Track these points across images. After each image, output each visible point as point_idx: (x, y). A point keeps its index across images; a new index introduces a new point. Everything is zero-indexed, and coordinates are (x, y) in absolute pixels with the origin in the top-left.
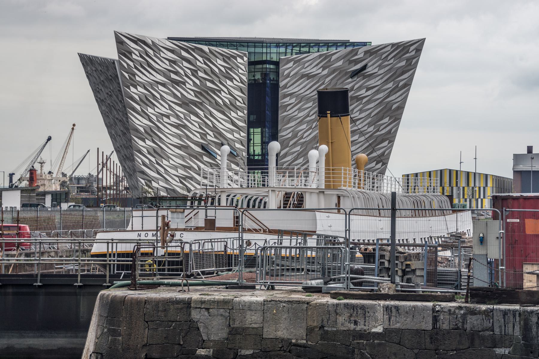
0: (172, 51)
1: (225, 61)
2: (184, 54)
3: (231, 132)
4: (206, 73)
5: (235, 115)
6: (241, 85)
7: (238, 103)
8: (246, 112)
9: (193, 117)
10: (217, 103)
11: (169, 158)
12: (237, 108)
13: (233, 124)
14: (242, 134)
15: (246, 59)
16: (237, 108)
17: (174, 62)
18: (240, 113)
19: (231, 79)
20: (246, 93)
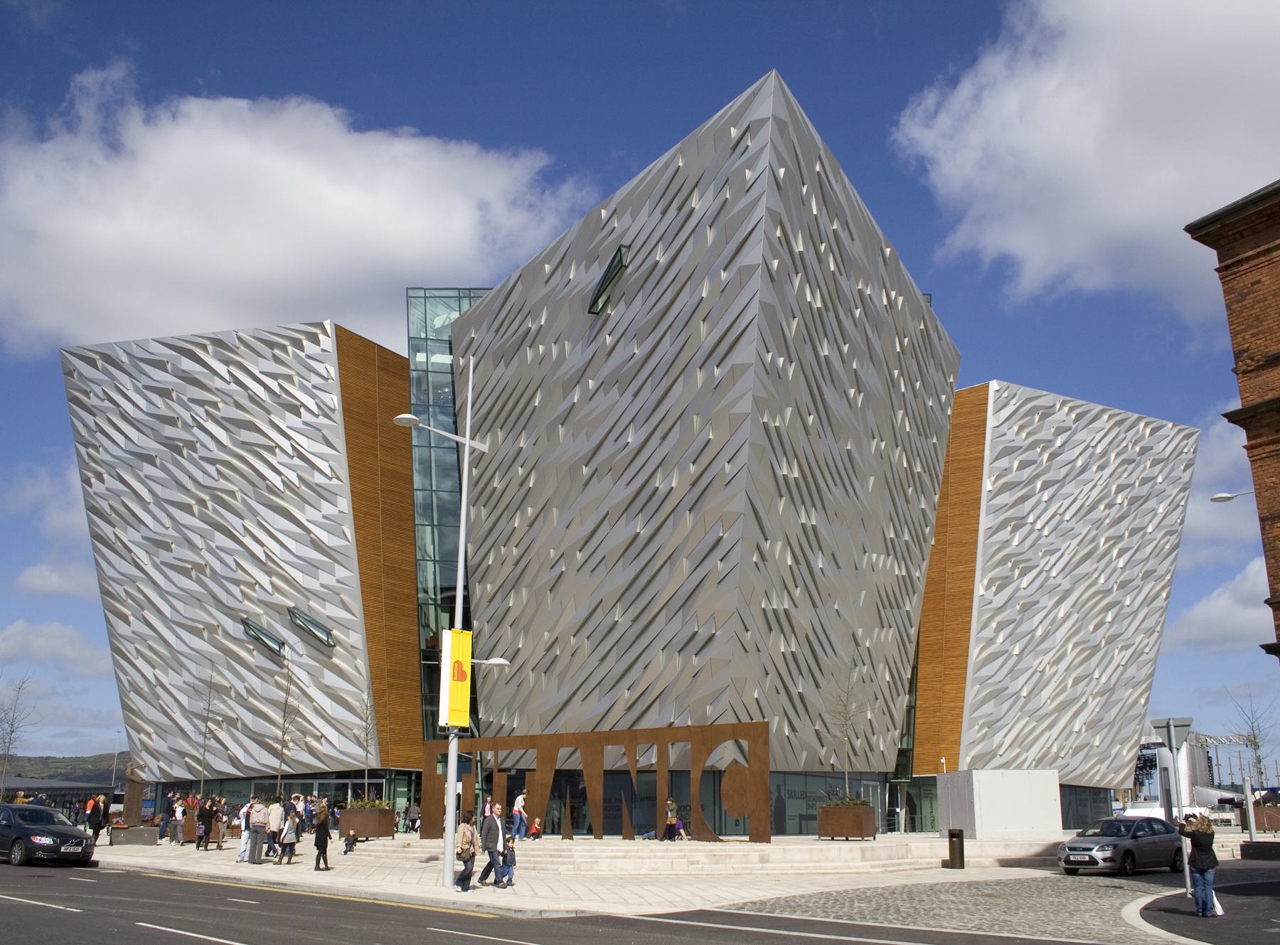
0: (160, 365)
1: (277, 360)
2: (187, 365)
3: (311, 568)
4: (238, 406)
5: (317, 516)
6: (322, 420)
7: (318, 479)
8: (344, 504)
9: (221, 540)
10: (272, 489)
11: (182, 665)
12: (322, 493)
13: (317, 545)
14: (341, 572)
15: (328, 343)
16: (322, 493)
17: (165, 393)
18: (327, 508)
19: (295, 410)
20: (340, 442)
